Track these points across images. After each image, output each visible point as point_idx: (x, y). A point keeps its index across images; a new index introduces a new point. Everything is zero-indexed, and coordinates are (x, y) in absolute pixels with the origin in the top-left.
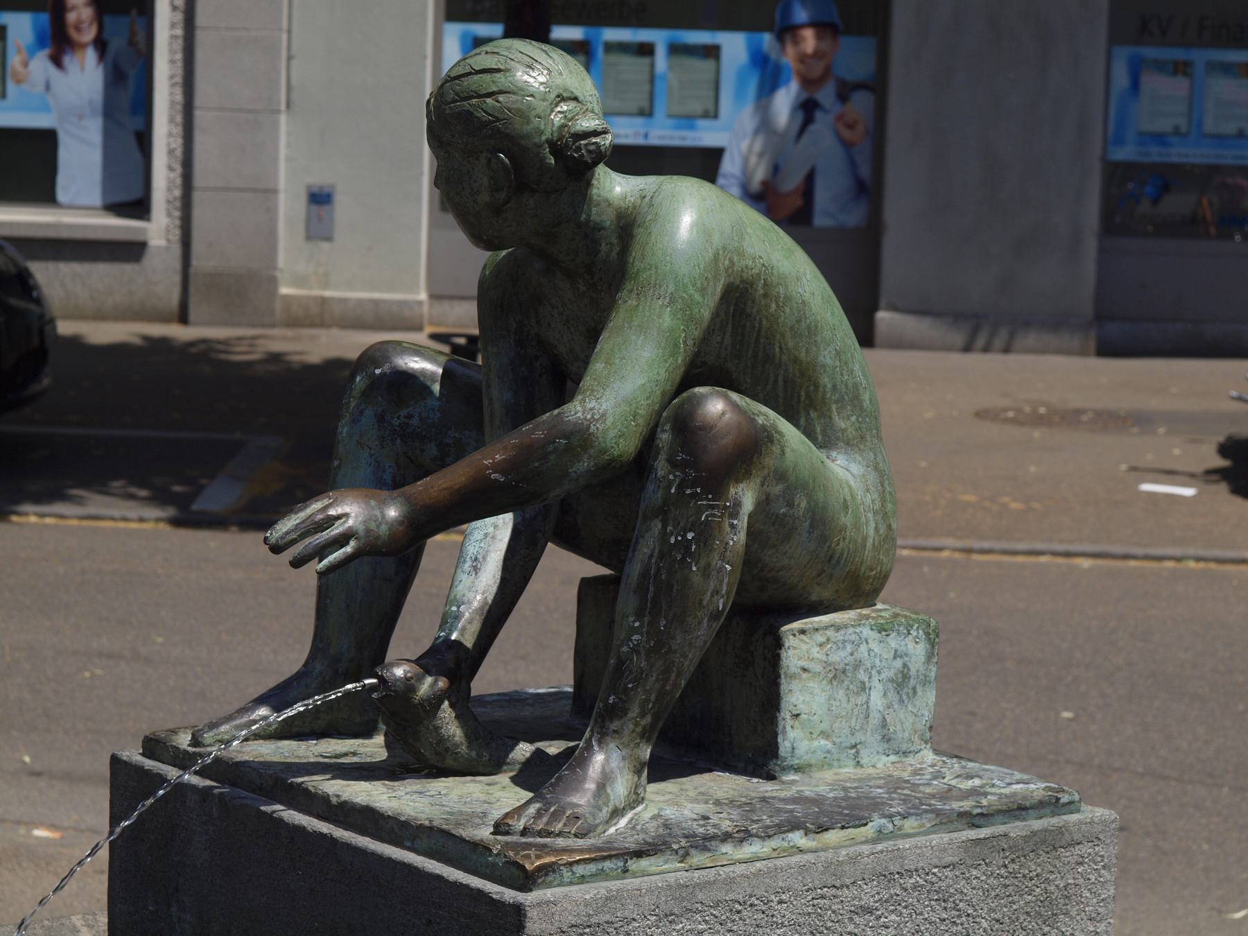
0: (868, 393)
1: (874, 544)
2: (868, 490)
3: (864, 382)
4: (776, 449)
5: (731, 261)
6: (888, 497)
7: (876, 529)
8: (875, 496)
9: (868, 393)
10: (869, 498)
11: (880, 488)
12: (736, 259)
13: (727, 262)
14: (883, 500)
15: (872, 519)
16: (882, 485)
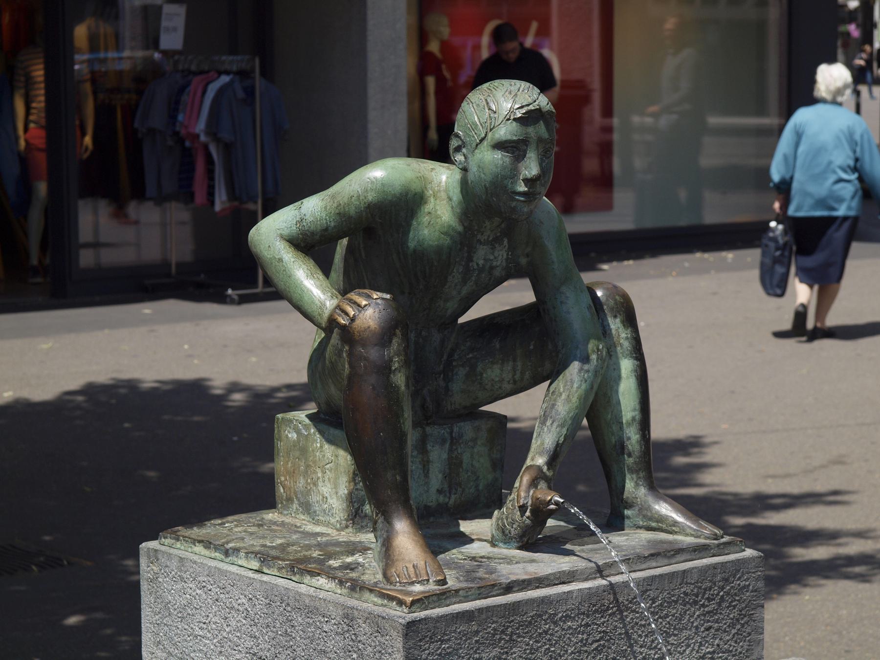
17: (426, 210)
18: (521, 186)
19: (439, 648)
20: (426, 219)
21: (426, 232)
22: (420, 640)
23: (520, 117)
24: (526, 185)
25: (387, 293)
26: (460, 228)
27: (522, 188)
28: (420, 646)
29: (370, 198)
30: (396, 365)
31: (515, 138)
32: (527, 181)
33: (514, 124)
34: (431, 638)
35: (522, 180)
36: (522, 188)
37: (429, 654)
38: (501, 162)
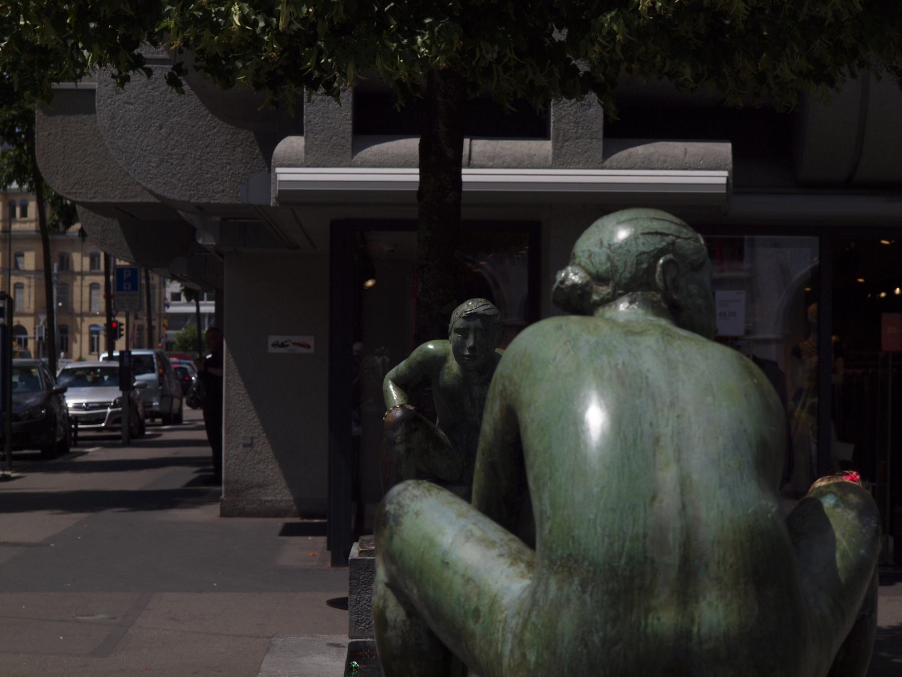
0: (550, 523)
1: (509, 666)
2: (519, 613)
3: (549, 512)
4: (386, 533)
5: (504, 386)
6: (529, 626)
7: (512, 651)
8: (521, 621)
9: (550, 523)
10: (513, 623)
11: (526, 615)
12: (507, 384)
13: (501, 386)
14: (525, 625)
15: (510, 640)
16: (529, 613)
17: (447, 366)
18: (466, 352)
19: (370, 575)
20: (447, 371)
21: (446, 377)
22: (359, 569)
23: (465, 316)
24: (469, 352)
25: (412, 405)
26: (462, 376)
27: (467, 353)
28: (359, 572)
29: (419, 359)
30: (399, 440)
31: (462, 327)
32: (470, 349)
33: (462, 320)
34: (365, 569)
35: (468, 349)
36: (467, 353)
37: (364, 577)
38: (456, 339)
